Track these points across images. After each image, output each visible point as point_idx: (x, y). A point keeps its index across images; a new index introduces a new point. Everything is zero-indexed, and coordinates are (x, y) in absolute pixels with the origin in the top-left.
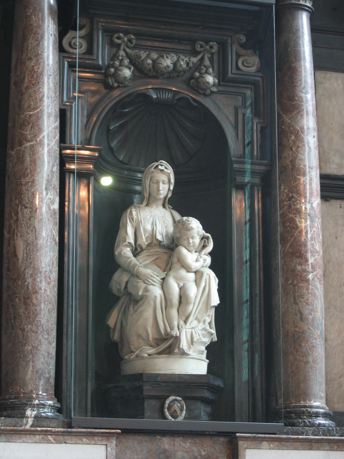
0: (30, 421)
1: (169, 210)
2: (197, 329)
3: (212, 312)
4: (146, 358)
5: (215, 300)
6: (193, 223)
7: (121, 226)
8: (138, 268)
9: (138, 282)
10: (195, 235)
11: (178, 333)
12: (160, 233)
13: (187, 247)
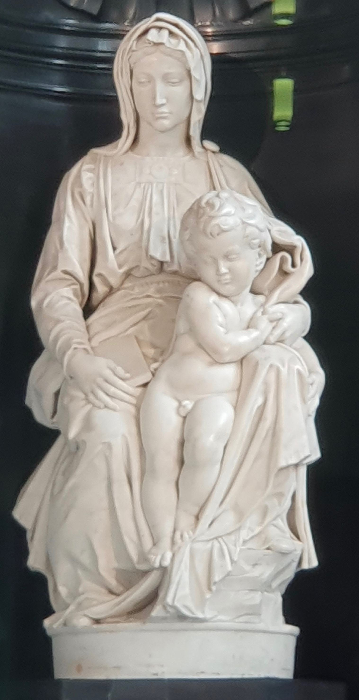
1: (203, 158)
2: (233, 537)
4: (84, 631)
6: (225, 211)
7: (54, 217)
8: (73, 356)
9: (72, 399)
10: (236, 247)
11: (169, 555)
12: (164, 238)
13: (216, 286)
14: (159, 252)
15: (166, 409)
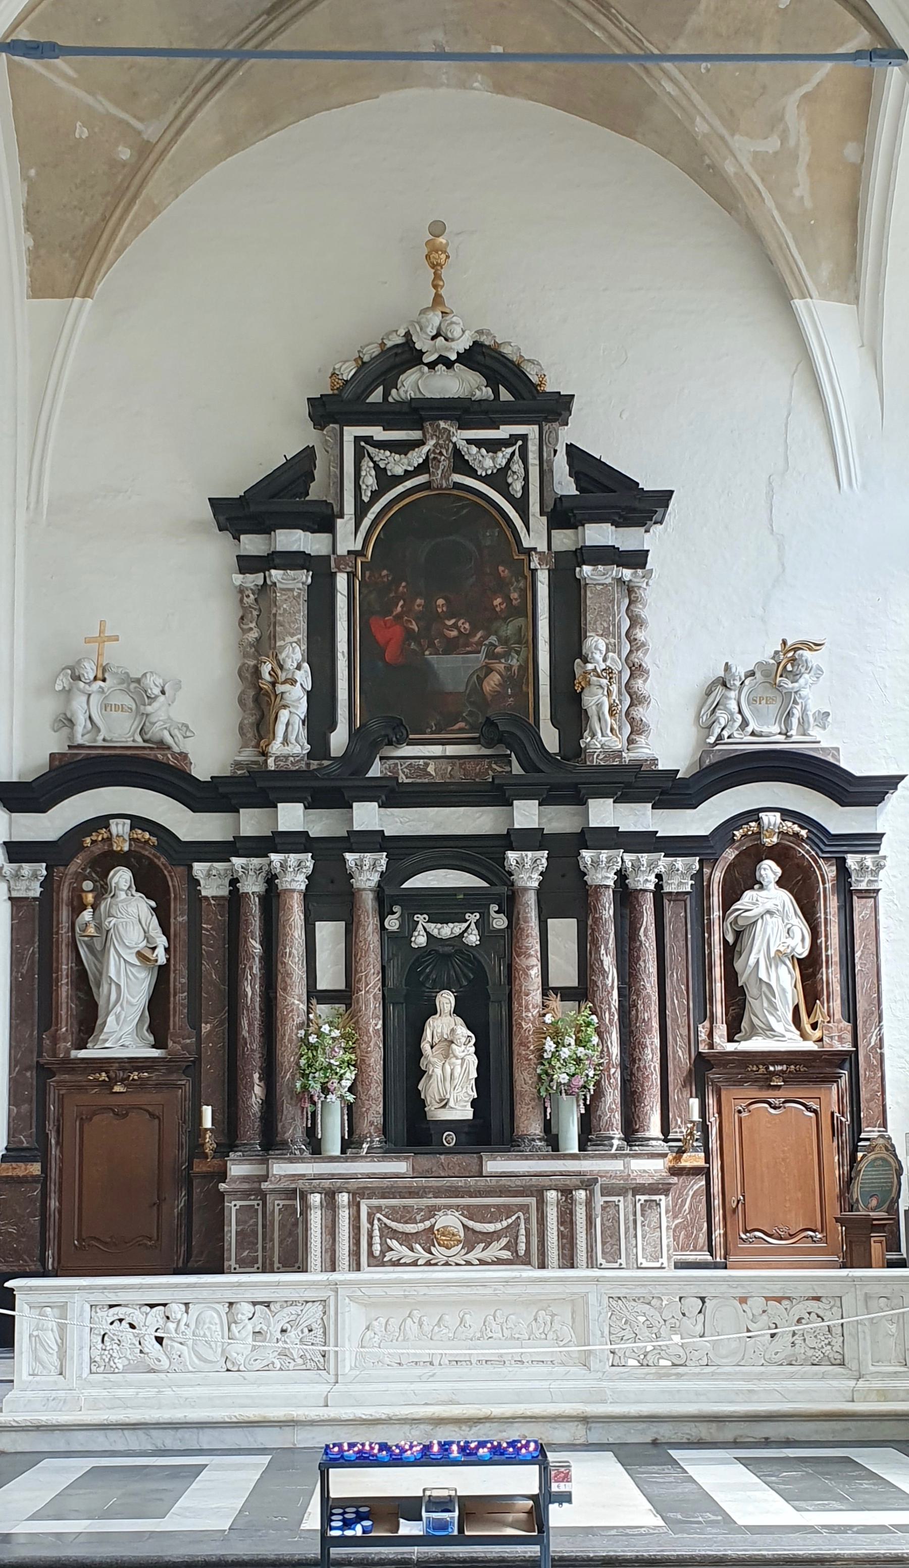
0: (365, 1150)
3: (473, 1082)
5: (474, 1075)
14: (445, 1037)
15: (448, 1068)
